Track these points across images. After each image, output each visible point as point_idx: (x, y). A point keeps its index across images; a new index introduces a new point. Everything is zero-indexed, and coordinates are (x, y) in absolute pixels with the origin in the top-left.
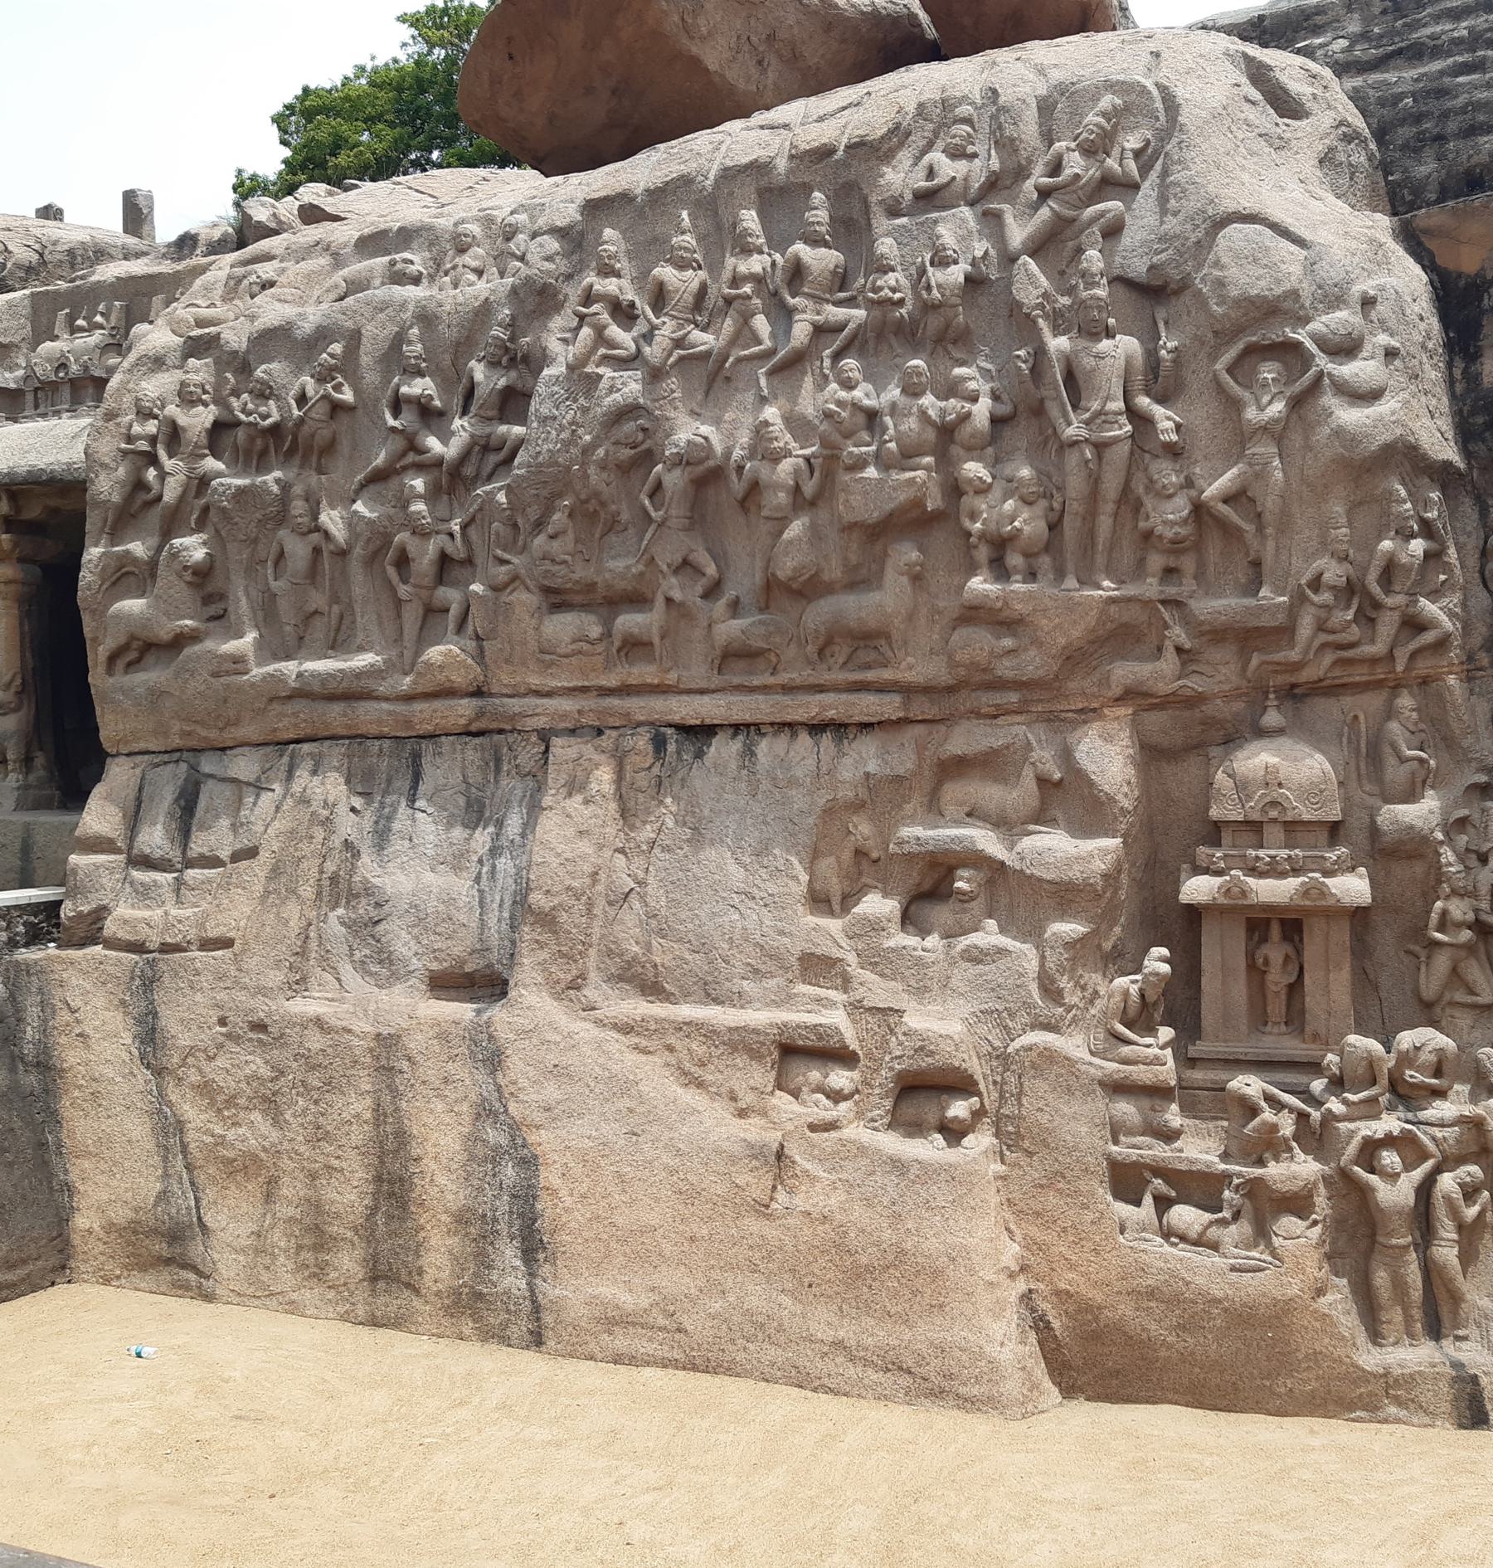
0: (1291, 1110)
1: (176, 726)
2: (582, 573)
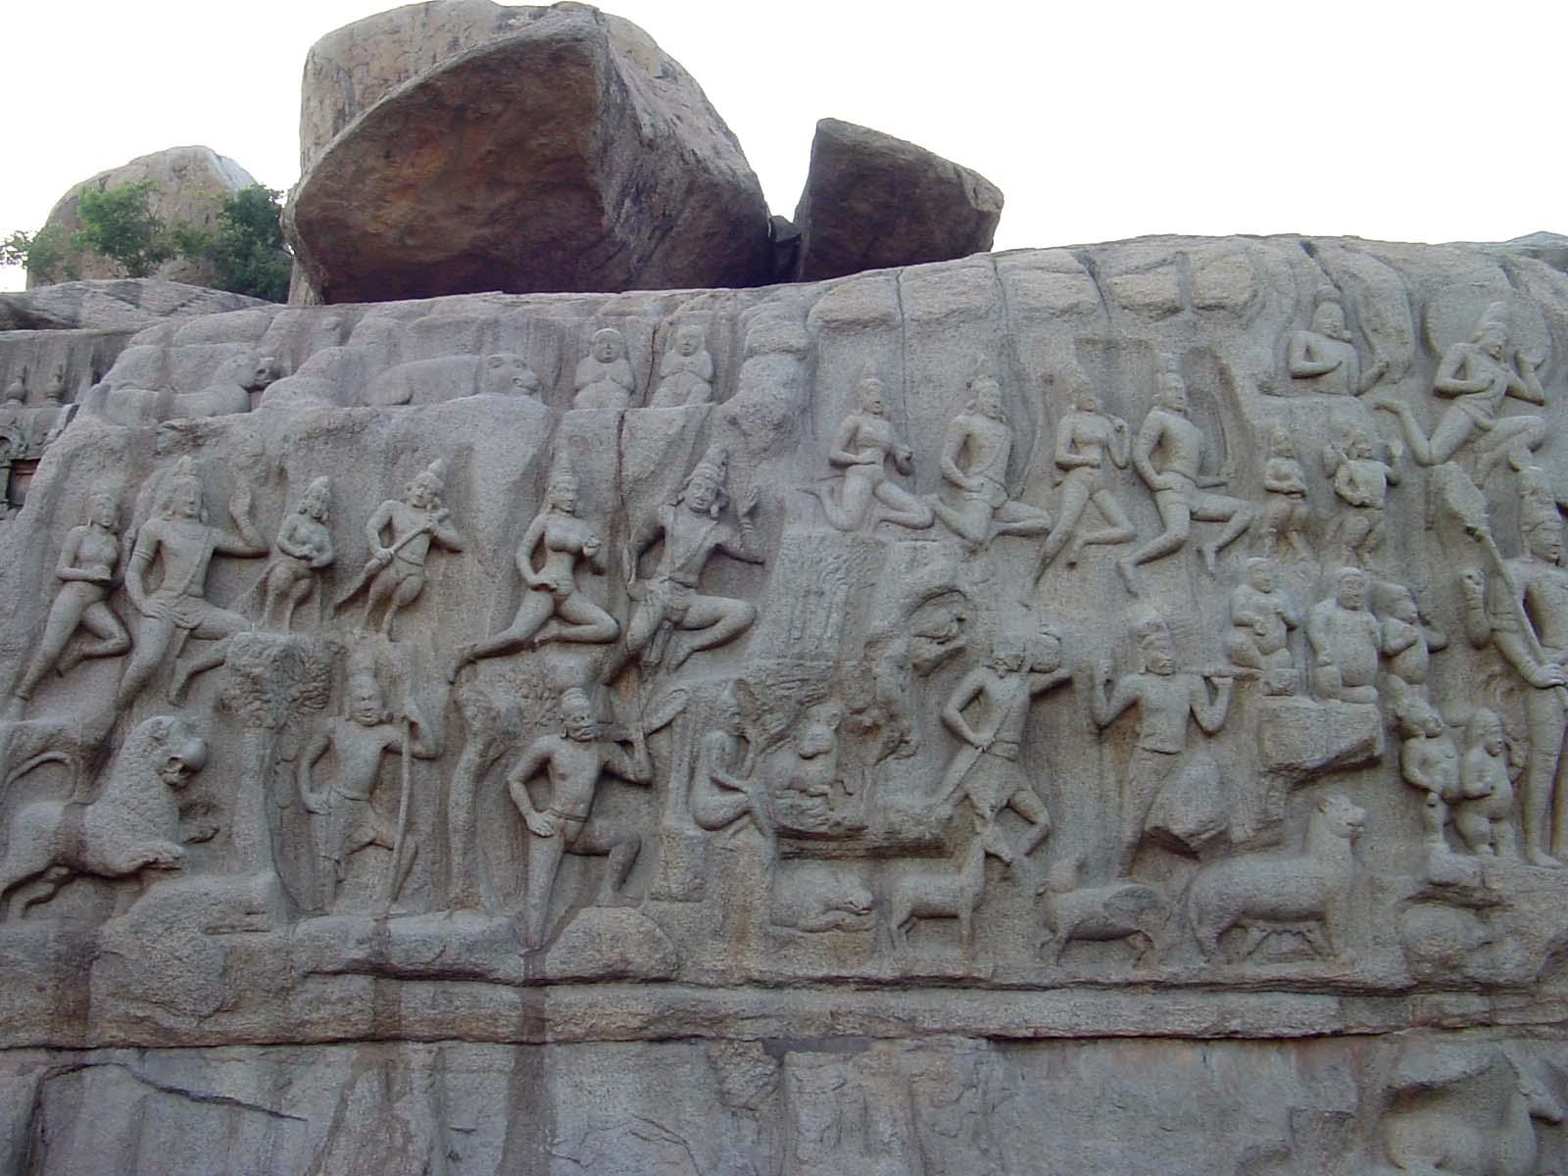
1: (122, 1007)
2: (849, 813)
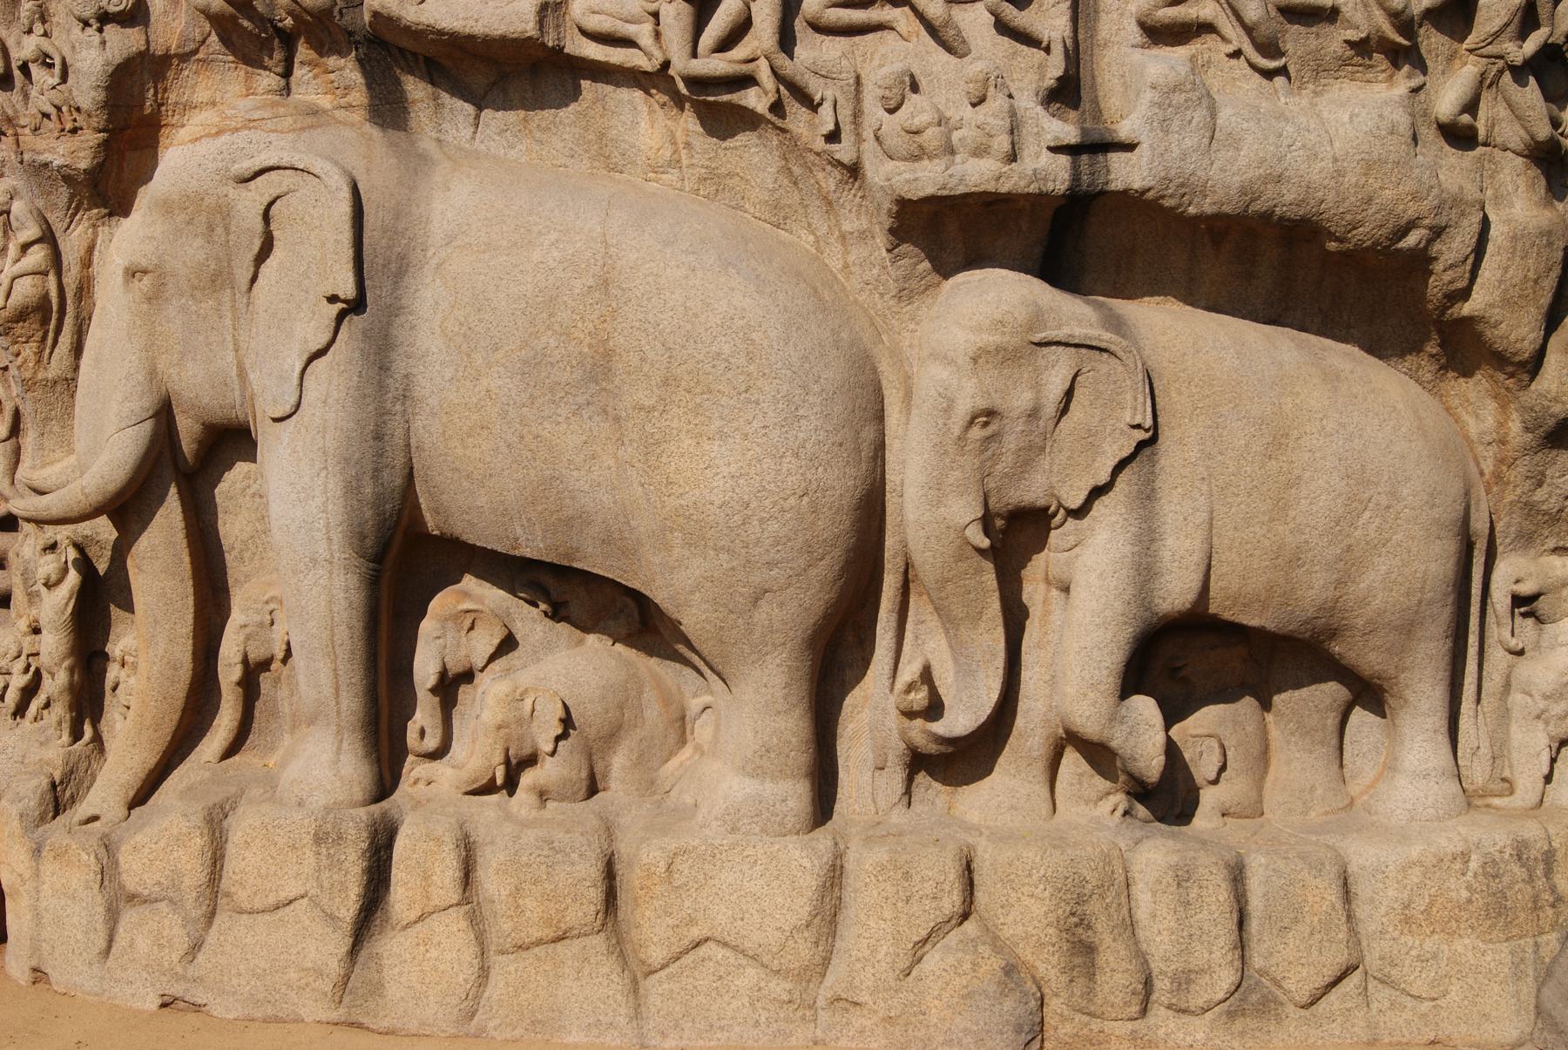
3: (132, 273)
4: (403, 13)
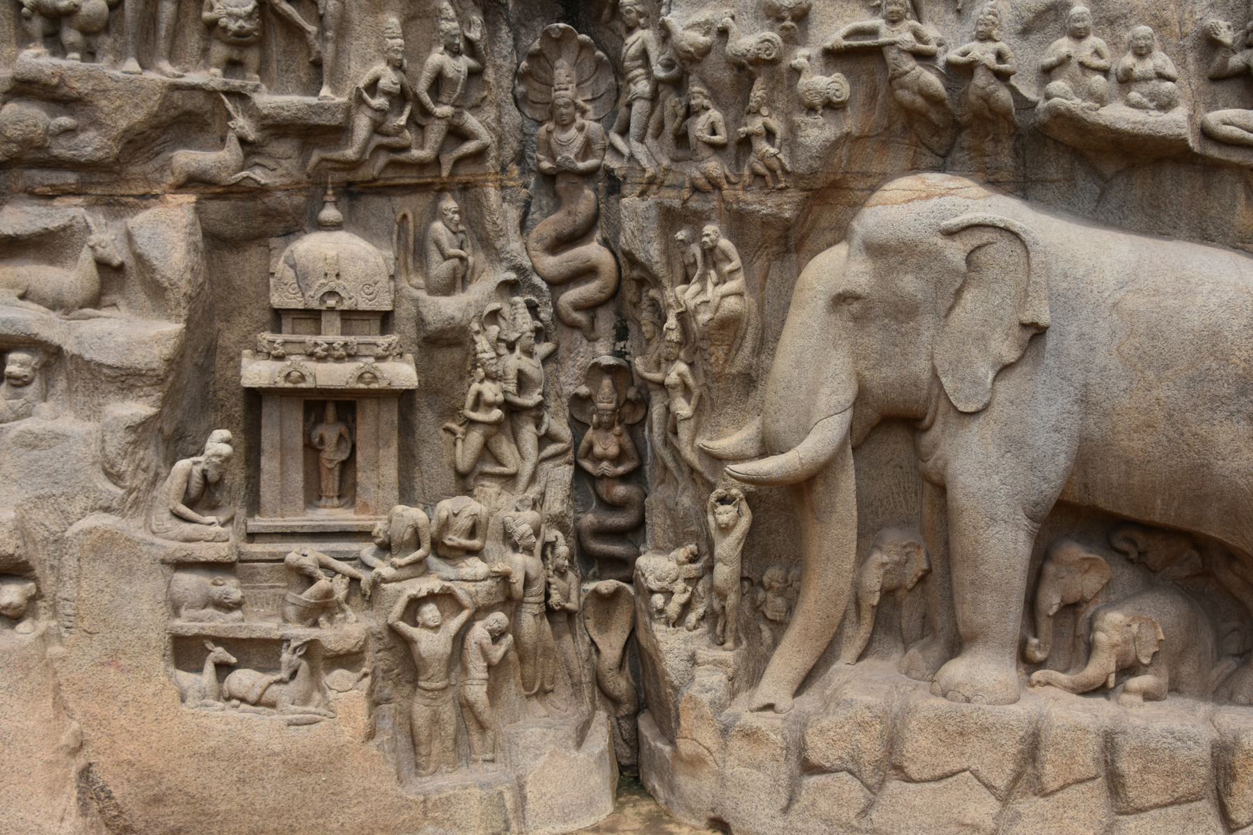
0: (344, 576)
3: (841, 300)
4: (1084, 116)
